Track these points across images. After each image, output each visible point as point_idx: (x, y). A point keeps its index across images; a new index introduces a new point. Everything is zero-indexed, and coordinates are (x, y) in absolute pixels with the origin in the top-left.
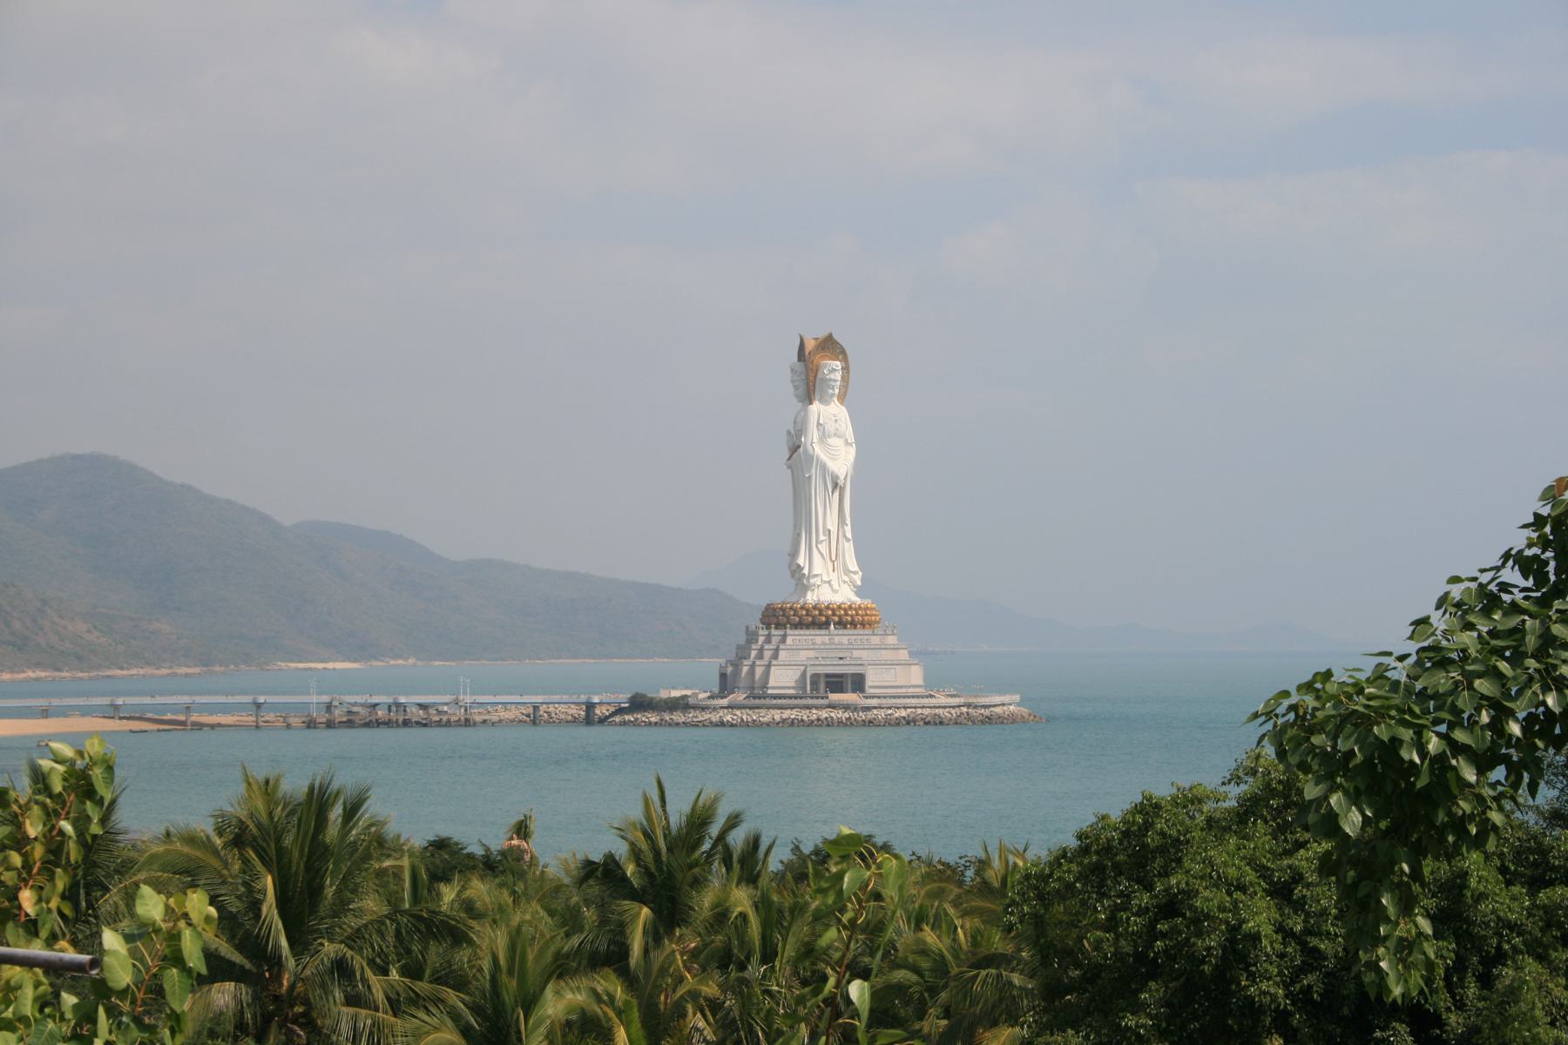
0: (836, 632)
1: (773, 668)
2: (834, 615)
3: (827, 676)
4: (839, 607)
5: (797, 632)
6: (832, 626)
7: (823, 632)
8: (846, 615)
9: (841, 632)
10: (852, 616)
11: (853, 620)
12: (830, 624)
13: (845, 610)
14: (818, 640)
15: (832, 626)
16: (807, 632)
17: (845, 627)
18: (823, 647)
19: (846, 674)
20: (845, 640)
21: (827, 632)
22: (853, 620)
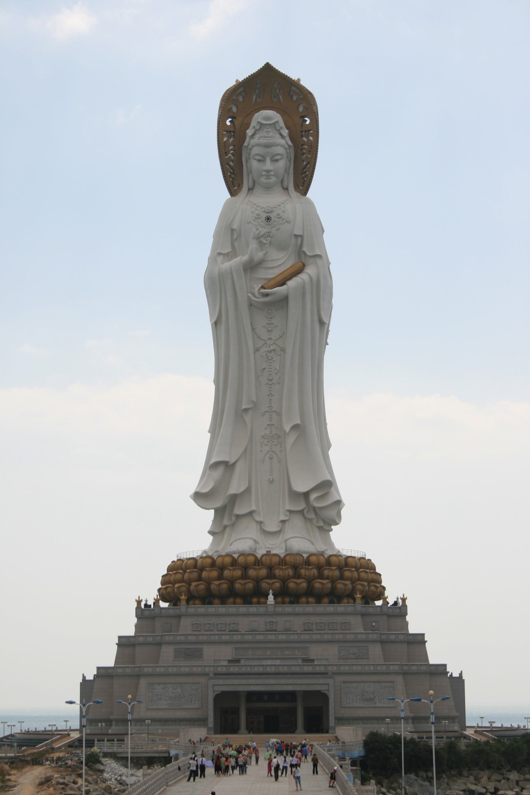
0: (279, 609)
1: (143, 682)
2: (297, 576)
3: (251, 696)
4: (307, 563)
5: (201, 609)
6: (271, 598)
7: (253, 609)
8: (321, 576)
9: (289, 608)
10: (353, 581)
11: (333, 588)
12: (266, 596)
13: (319, 567)
14: (244, 624)
15: (271, 598)
16: (243, 609)
17: (319, 600)
18: (249, 638)
19: (291, 696)
20: (297, 623)
21: (262, 609)
22: (333, 588)
